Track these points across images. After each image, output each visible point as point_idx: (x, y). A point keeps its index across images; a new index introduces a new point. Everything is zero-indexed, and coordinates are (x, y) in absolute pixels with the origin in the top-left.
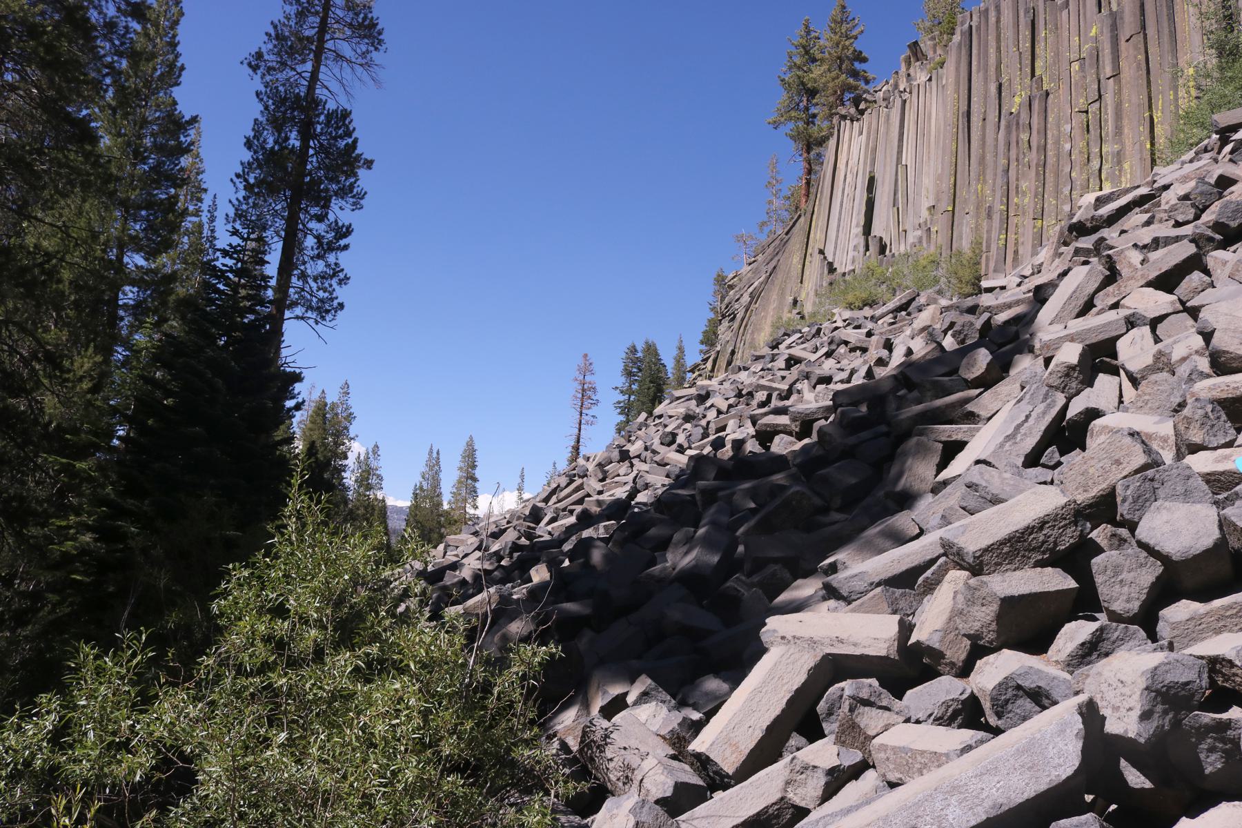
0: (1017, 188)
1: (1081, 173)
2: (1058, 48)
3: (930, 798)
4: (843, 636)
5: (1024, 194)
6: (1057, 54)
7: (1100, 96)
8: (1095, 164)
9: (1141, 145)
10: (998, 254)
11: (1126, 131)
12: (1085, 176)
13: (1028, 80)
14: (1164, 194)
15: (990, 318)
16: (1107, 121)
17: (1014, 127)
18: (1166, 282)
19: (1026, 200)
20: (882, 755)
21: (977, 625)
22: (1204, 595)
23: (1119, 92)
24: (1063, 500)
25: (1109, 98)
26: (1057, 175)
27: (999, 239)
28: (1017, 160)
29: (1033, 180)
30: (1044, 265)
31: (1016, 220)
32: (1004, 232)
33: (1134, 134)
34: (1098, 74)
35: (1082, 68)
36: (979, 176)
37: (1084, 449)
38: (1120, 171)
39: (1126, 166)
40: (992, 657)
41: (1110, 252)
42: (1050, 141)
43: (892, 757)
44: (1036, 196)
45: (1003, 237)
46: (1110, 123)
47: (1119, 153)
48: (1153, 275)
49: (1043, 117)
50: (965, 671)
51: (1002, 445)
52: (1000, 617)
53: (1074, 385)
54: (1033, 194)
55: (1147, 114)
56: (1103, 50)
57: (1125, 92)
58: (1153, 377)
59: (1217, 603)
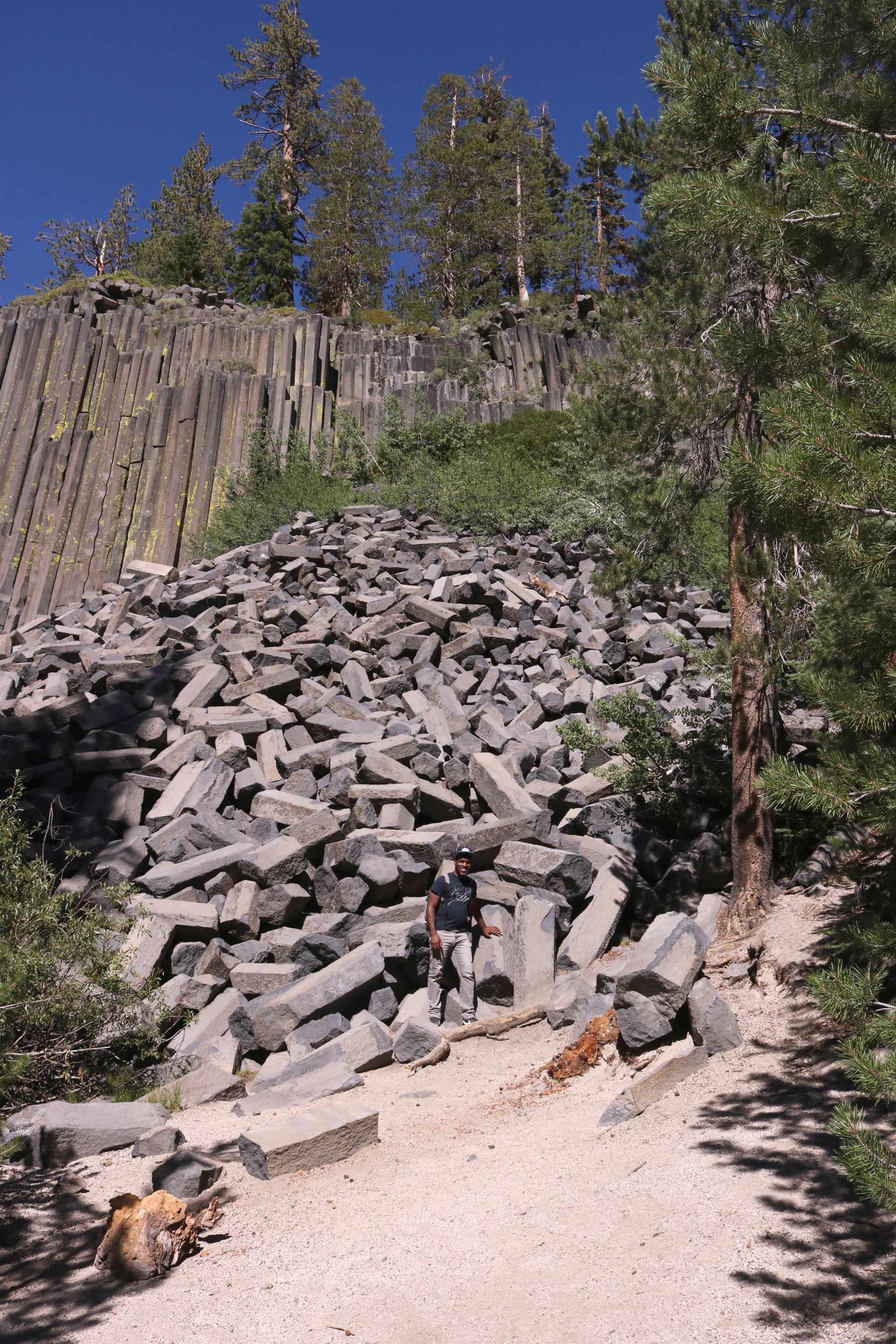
0: (41, 515)
1: (111, 525)
3: (330, 980)
4: (184, 914)
5: (47, 523)
6: (110, 401)
7: (143, 459)
8: (125, 520)
10: (8, 575)
11: (160, 501)
12: (113, 529)
13: (74, 414)
14: (240, 604)
15: (106, 677)
16: (144, 484)
17: (51, 455)
18: (279, 694)
19: (49, 531)
20: (239, 979)
21: (272, 912)
22: (384, 904)
23: (160, 463)
24: (300, 846)
25: (151, 464)
26: (84, 518)
27: (12, 561)
28: (48, 488)
30: (110, 624)
33: (167, 507)
34: (145, 438)
35: (132, 425)
37: (247, 810)
38: (147, 535)
39: (154, 533)
40: (276, 931)
41: (226, 654)
42: (85, 482)
43: (246, 979)
44: (60, 531)
45: (17, 559)
46: (147, 487)
47: (149, 518)
48: (267, 686)
49: (82, 456)
50: (258, 938)
51: (202, 800)
52: (288, 908)
53: (240, 764)
56: (155, 418)
57: (167, 466)
58: (301, 771)
59: (391, 908)
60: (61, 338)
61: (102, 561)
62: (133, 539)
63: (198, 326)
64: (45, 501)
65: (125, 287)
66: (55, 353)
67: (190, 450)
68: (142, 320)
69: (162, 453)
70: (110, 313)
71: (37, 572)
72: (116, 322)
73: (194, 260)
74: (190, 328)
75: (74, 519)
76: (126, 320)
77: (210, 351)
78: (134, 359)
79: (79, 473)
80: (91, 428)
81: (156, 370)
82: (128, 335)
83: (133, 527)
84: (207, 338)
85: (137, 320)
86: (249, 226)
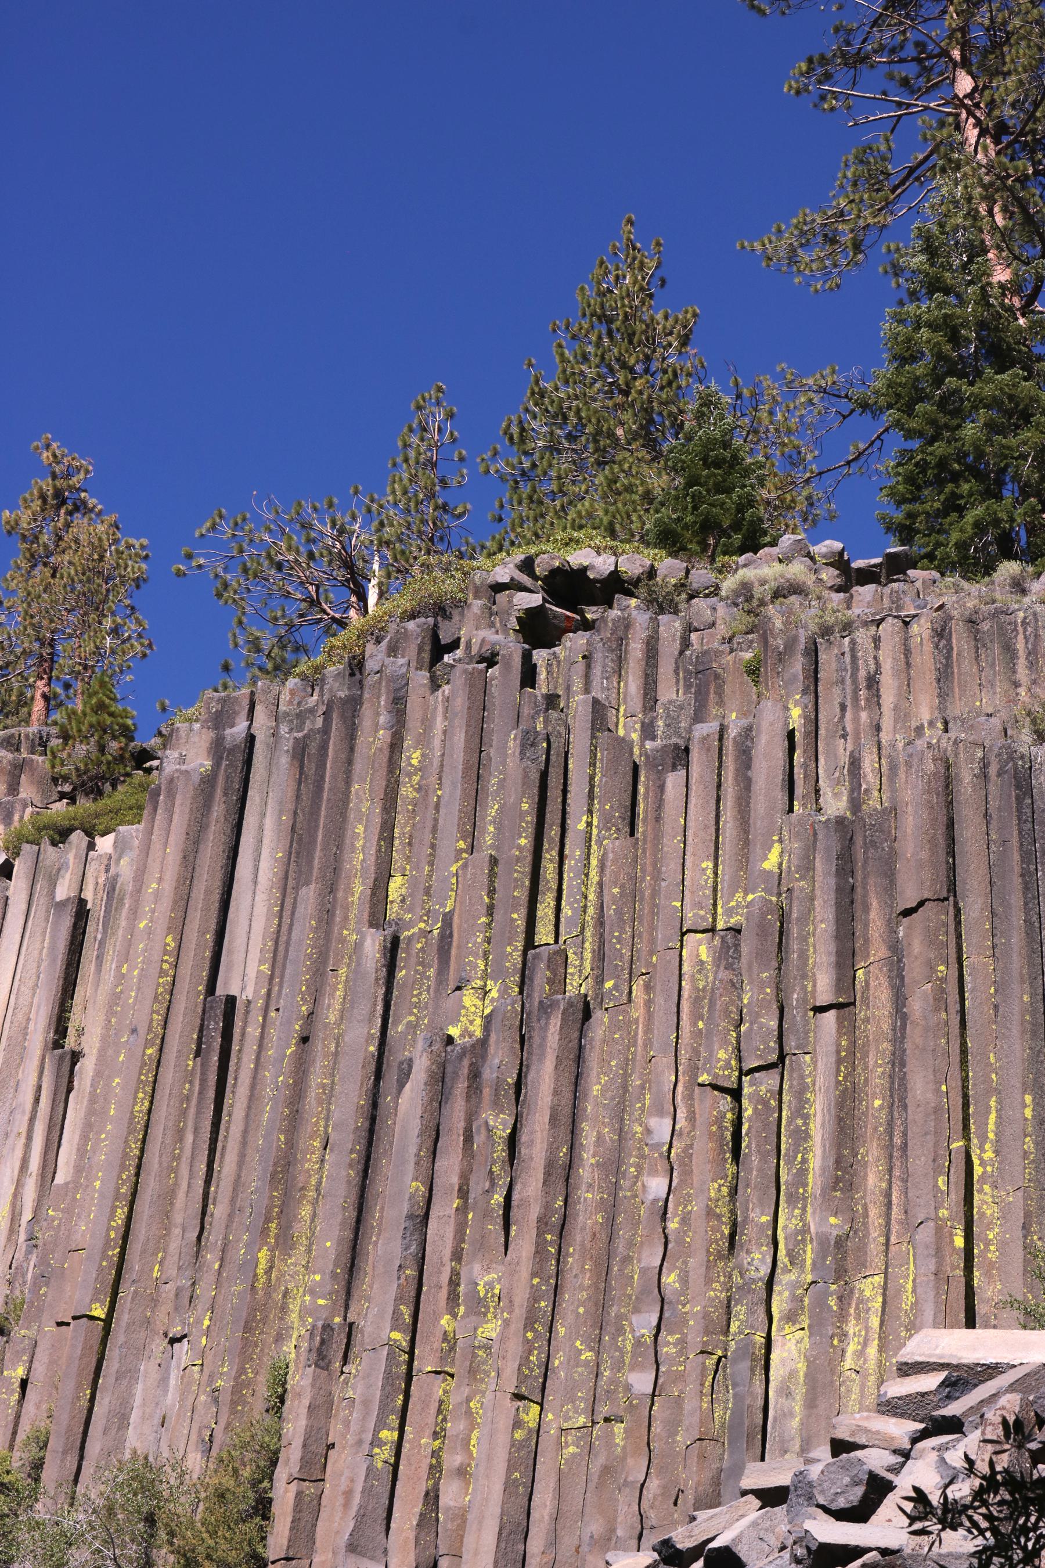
0: (454, 1282)
1: (709, 1281)
2: (634, 879)
5: (479, 1307)
6: (632, 894)
7: (782, 1057)
9: (939, 1230)
12: (717, 1292)
13: (514, 951)
16: (802, 1136)
17: (461, 1086)
19: (490, 1329)
26: (604, 1272)
27: (376, 1442)
28: (463, 1193)
29: (525, 1269)
31: (439, 1388)
32: (394, 1420)
36: (268, 1220)
42: (588, 1158)
44: (529, 1323)
45: (389, 1435)
47: (840, 1243)
49: (568, 1077)
54: (520, 1312)
55: (958, 1144)
60: (424, 740)
61: (694, 1405)
62: (791, 1317)
63: (890, 626)
64: (460, 1236)
65: (601, 564)
66: (407, 791)
67: (953, 997)
68: (686, 643)
69: (848, 1028)
70: (575, 642)
71: (462, 1472)
72: (602, 662)
73: (741, 509)
74: (863, 636)
75: (570, 1280)
76: (636, 649)
77: (943, 695)
78: (695, 755)
79: (564, 1132)
80: (577, 985)
81: (780, 777)
82: (650, 699)
83: (784, 1280)
84: (925, 658)
85: (669, 648)
86: (919, 369)
